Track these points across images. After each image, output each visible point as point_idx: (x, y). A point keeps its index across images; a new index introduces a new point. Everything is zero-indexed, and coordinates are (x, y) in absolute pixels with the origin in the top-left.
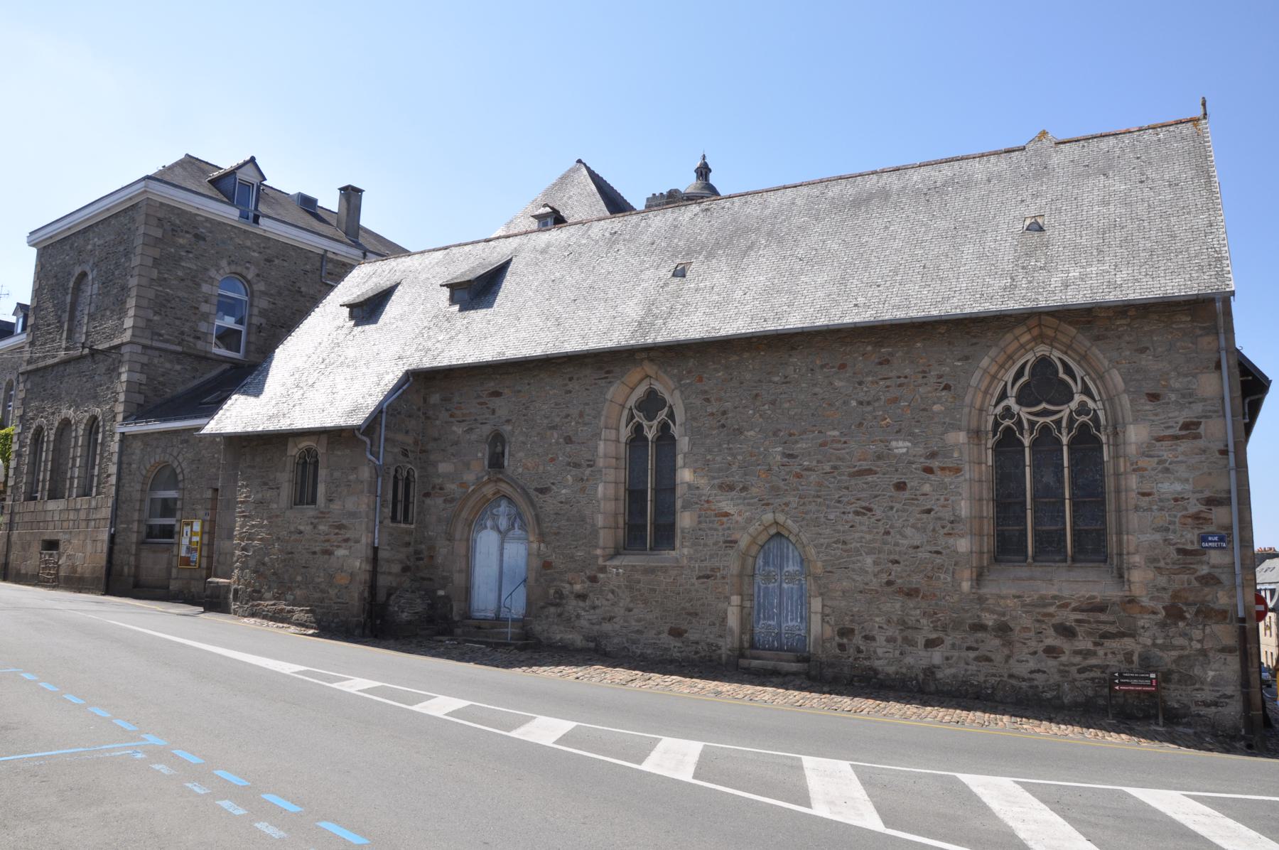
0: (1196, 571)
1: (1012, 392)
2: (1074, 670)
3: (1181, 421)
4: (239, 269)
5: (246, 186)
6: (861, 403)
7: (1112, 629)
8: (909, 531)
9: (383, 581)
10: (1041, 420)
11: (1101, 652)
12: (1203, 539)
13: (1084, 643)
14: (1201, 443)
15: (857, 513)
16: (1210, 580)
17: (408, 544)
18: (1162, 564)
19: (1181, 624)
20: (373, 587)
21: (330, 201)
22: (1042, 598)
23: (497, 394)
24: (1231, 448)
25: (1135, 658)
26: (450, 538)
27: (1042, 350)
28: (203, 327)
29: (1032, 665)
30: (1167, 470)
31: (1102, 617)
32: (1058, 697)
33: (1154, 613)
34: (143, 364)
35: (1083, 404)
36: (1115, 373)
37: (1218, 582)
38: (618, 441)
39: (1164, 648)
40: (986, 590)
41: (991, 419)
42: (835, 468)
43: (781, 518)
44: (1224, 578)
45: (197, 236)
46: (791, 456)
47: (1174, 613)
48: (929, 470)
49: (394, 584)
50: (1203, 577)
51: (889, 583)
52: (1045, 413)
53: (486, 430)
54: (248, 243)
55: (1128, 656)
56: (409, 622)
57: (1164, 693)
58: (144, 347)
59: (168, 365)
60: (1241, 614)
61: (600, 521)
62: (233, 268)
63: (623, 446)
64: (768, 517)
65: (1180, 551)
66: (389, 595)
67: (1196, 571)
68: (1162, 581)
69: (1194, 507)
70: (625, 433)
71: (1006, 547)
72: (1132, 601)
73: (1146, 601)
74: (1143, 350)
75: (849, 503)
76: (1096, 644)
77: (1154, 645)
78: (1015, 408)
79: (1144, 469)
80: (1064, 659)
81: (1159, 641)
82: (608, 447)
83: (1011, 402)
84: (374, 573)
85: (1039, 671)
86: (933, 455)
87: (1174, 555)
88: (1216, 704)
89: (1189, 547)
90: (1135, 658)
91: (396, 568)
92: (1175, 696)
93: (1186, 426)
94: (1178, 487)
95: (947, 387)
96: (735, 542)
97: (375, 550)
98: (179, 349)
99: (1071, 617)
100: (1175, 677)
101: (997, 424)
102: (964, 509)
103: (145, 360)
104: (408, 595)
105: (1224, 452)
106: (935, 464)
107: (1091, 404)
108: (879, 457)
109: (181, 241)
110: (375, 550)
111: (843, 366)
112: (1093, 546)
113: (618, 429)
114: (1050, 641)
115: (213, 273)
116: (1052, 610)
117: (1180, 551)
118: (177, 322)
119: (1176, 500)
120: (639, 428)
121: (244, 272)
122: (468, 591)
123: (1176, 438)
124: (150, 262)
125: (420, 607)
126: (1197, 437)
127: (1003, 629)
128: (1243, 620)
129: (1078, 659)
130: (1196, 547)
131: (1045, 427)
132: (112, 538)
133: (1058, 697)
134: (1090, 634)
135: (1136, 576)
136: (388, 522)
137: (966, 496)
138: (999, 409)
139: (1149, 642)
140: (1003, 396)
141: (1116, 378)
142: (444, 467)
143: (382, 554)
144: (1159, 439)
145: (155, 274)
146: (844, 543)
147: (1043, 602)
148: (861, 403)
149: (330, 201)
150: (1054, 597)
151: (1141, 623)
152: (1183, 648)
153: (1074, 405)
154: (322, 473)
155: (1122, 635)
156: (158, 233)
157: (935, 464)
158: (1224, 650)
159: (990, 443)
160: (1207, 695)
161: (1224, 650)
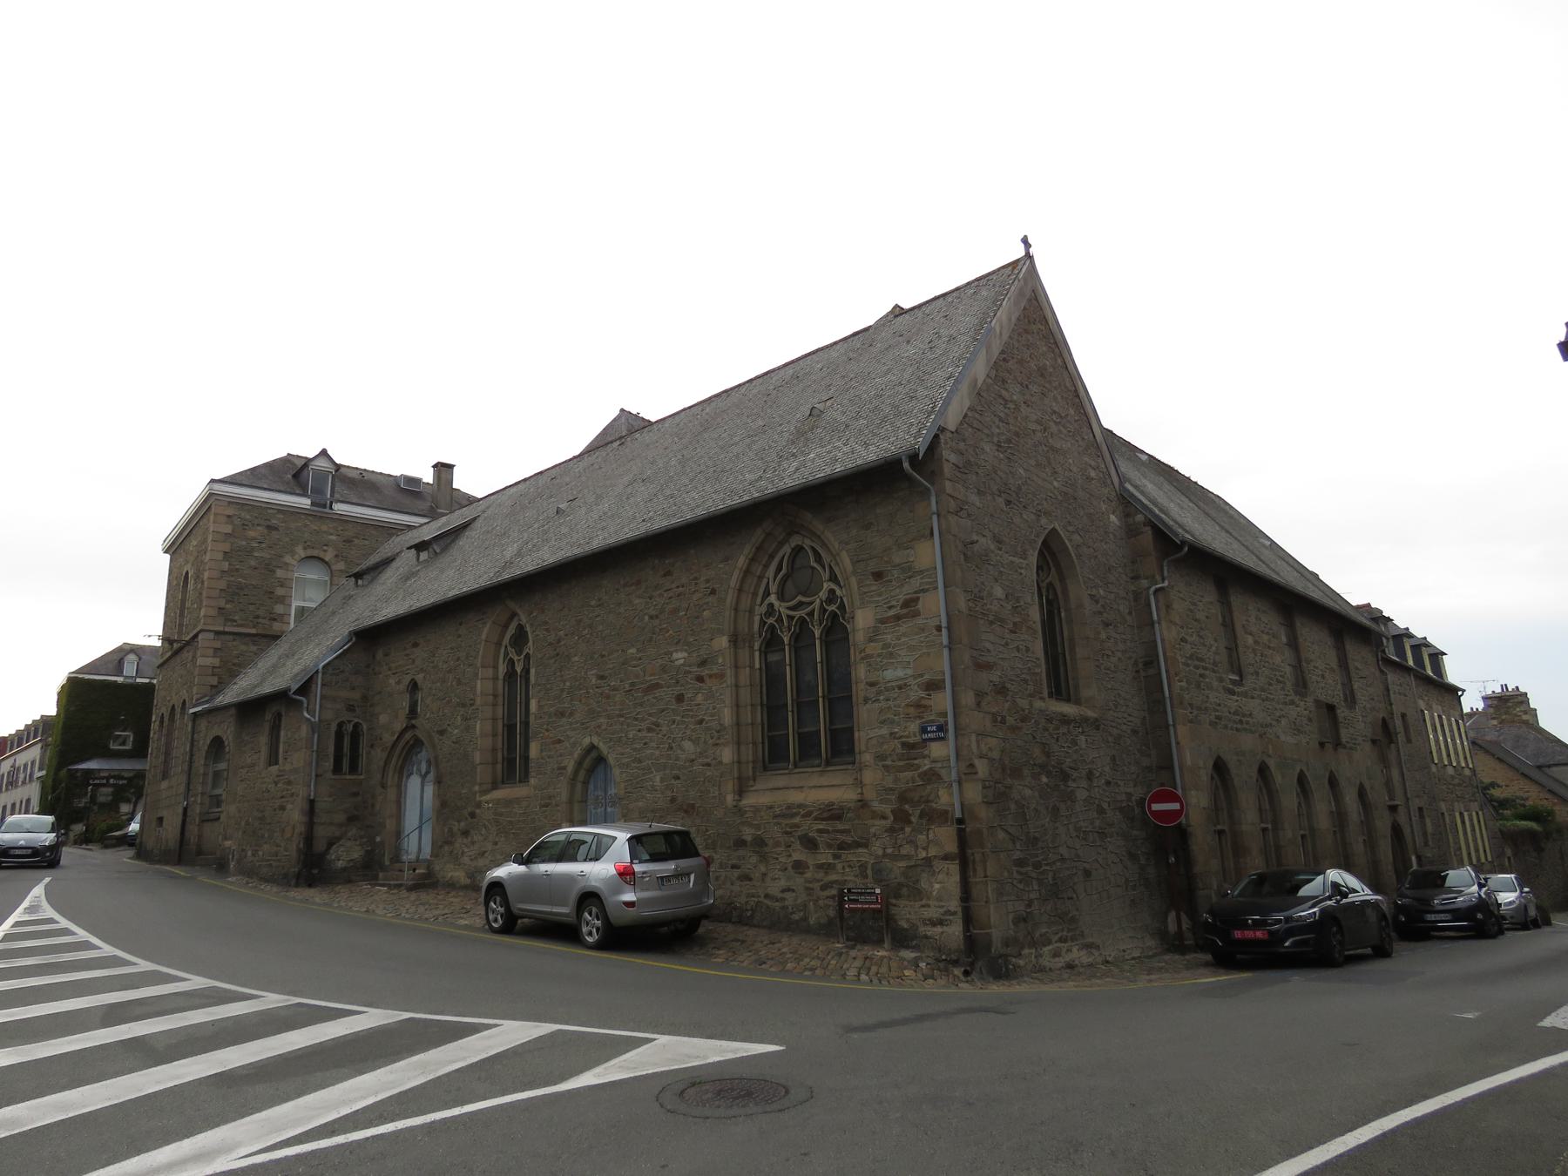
0: (919, 767)
1: (773, 588)
2: (817, 886)
3: (902, 597)
4: (315, 553)
5: (321, 476)
6: (651, 617)
7: (849, 839)
8: (687, 745)
9: (322, 832)
10: (797, 614)
11: (839, 866)
12: (924, 730)
13: (825, 856)
14: (919, 621)
15: (649, 730)
16: (932, 776)
17: (356, 794)
18: (889, 762)
19: (908, 830)
20: (309, 838)
21: (428, 477)
22: (789, 807)
23: (416, 645)
24: (944, 624)
25: (869, 872)
26: (383, 786)
27: (796, 541)
28: (279, 609)
29: (783, 883)
30: (891, 655)
31: (840, 826)
32: (805, 919)
33: (884, 818)
34: (216, 649)
35: (832, 591)
36: (844, 554)
37: (939, 777)
38: (495, 678)
39: (895, 857)
40: (749, 800)
41: (757, 619)
42: (632, 684)
43: (595, 741)
44: (943, 772)
45: (269, 527)
46: (602, 678)
47: (901, 817)
48: (700, 679)
49: (337, 834)
50: (925, 773)
51: (673, 800)
52: (800, 605)
53: (407, 679)
54: (324, 528)
55: (863, 867)
56: (344, 869)
57: (894, 910)
58: (217, 633)
59: (243, 648)
60: (958, 815)
61: (477, 758)
63: (500, 683)
64: (587, 741)
65: (904, 745)
66: (330, 844)
67: (919, 767)
68: (889, 782)
69: (916, 693)
70: (502, 669)
71: (774, 756)
72: (863, 804)
73: (876, 806)
74: (867, 527)
75: (643, 720)
76: (836, 857)
77: (885, 855)
78: (777, 604)
79: (870, 656)
80: (808, 875)
81: (889, 851)
82: (484, 685)
83: (773, 598)
84: (311, 825)
85: (788, 890)
86: (703, 663)
87: (899, 750)
88: (941, 923)
89: (911, 740)
90: (869, 872)
91: (340, 817)
92: (906, 913)
93: (906, 604)
94: (900, 673)
95: (713, 592)
96: (565, 768)
97: (312, 802)
98: (253, 631)
99: (812, 827)
100: (904, 891)
101: (763, 623)
102: (727, 716)
103: (218, 644)
104: (349, 844)
105: (939, 629)
106: (705, 672)
107: (838, 592)
108: (664, 669)
109: (251, 534)
110: (312, 802)
111: (639, 583)
112: (842, 748)
113: (496, 667)
114: (796, 856)
115: (288, 559)
116: (797, 820)
117: (904, 745)
118: (252, 608)
119: (900, 688)
120: (512, 662)
121: (321, 555)
122: (399, 834)
123: (898, 618)
124: (220, 556)
125: (357, 854)
126: (916, 614)
127: (760, 842)
128: (960, 821)
129: (820, 875)
130: (918, 739)
131: (802, 621)
132: (185, 810)
133: (805, 919)
134: (830, 846)
135: (869, 776)
136: (330, 775)
137: (726, 702)
138: (764, 609)
139: (880, 852)
140: (767, 594)
141: (846, 559)
142: (383, 719)
143: (319, 806)
144: (883, 621)
145: (226, 566)
146: (640, 761)
147: (790, 811)
148: (651, 617)
149: (428, 477)
150: (800, 806)
151: (873, 830)
152: (908, 857)
153: (823, 594)
154: (282, 733)
155: (858, 845)
156: (228, 529)
157: (705, 672)
158: (946, 858)
159: (757, 646)
160: (933, 913)
161: (946, 858)
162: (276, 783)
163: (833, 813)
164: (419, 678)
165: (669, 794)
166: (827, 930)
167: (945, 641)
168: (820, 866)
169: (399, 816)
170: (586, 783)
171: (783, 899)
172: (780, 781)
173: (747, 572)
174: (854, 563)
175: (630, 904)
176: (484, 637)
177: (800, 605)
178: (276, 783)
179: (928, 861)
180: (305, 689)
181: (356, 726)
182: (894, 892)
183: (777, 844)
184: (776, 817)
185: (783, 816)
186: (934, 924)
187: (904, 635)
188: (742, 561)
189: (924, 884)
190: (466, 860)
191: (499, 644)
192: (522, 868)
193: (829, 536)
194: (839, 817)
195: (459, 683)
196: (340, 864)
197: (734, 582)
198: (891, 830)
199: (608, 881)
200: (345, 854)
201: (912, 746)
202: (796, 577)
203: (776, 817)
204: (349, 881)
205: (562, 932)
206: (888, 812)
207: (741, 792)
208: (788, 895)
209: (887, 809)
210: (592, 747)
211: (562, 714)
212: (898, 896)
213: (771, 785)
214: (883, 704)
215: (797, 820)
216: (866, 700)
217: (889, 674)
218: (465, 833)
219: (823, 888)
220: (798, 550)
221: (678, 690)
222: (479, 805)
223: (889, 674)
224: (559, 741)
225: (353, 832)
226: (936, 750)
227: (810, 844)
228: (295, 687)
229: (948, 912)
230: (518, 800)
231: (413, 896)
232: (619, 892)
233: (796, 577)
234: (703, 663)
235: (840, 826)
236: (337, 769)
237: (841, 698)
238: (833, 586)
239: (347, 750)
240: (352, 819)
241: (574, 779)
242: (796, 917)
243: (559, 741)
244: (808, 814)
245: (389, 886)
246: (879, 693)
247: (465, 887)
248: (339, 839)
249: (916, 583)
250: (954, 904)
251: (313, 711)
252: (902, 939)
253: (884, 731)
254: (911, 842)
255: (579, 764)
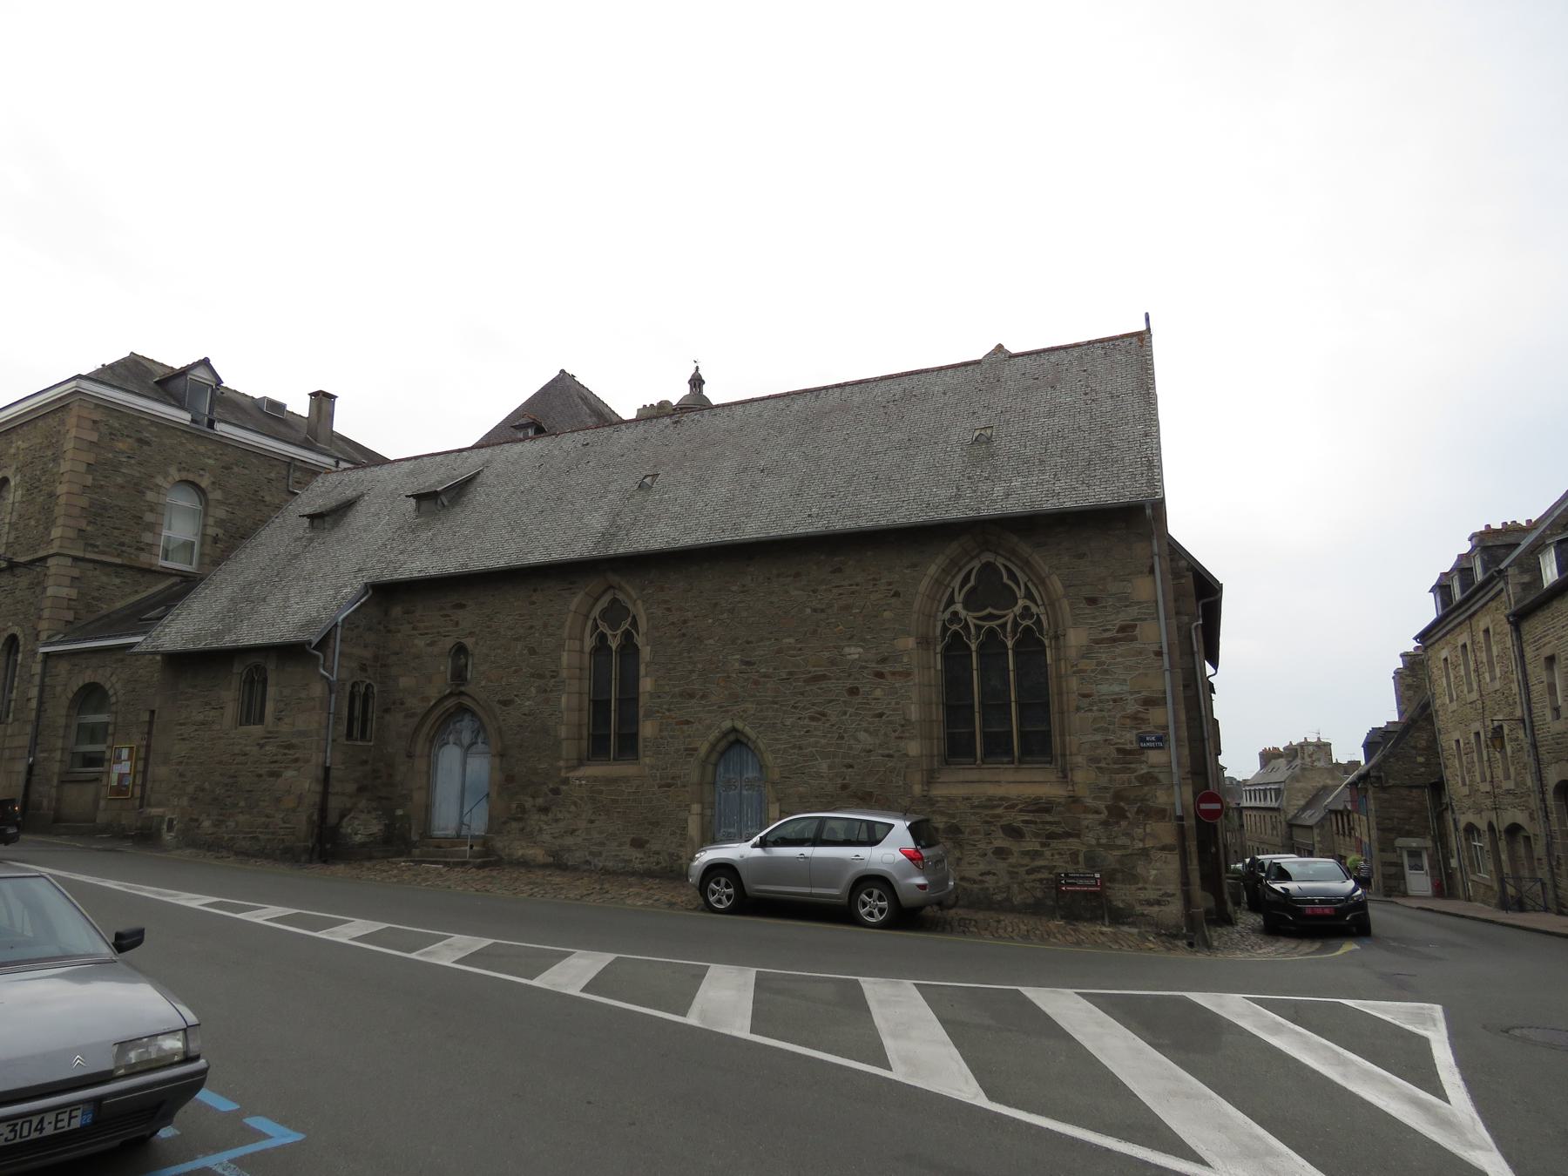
0: (1135, 770)
1: (959, 598)
2: (1022, 870)
3: (1118, 623)
4: (191, 477)
5: (200, 387)
6: (815, 610)
7: (1059, 830)
8: (862, 736)
9: (335, 803)
10: (987, 624)
11: (1048, 854)
12: (1142, 739)
13: (1032, 845)
14: (1136, 645)
15: (812, 719)
16: (1149, 779)
17: (365, 762)
18: (1103, 765)
19: (1124, 823)
20: (323, 809)
21: (299, 406)
22: (990, 799)
23: (462, 606)
24: (1165, 650)
25: (1081, 858)
26: (410, 756)
27: (988, 557)
28: (148, 537)
29: (982, 867)
30: (1106, 672)
31: (1049, 818)
32: (1008, 899)
33: (1097, 812)
34: (74, 579)
35: (1026, 608)
36: (1055, 578)
37: (1157, 781)
38: (582, 651)
39: (1109, 847)
40: (938, 791)
41: (939, 625)
42: (791, 673)
43: (739, 725)
44: (1161, 776)
45: (140, 441)
46: (748, 663)
47: (1116, 813)
48: (880, 675)
49: (349, 805)
50: (1142, 776)
51: (844, 787)
52: (990, 617)
53: (449, 643)
54: (202, 449)
55: (1075, 855)
56: (363, 845)
57: (1109, 892)
58: (75, 559)
59: (104, 579)
60: (1179, 813)
61: (563, 732)
62: (184, 475)
63: (587, 656)
64: (727, 724)
65: (1119, 751)
66: (342, 816)
67: (1135, 770)
68: (1104, 781)
69: (1132, 708)
70: (589, 643)
71: (957, 749)
72: (1074, 800)
73: (1089, 802)
74: (1081, 556)
75: (804, 708)
76: (1043, 845)
77: (1099, 845)
78: (963, 613)
79: (1084, 671)
80: (1012, 860)
81: (1103, 841)
82: (572, 657)
83: (958, 607)
84: (325, 794)
85: (989, 873)
86: (884, 660)
87: (1115, 755)
88: (1158, 903)
89: (1128, 747)
90: (1081, 858)
91: (351, 787)
92: (1121, 894)
93: (1122, 629)
94: (1116, 688)
95: (897, 594)
96: (695, 749)
97: (327, 770)
98: (118, 561)
99: (1018, 819)
100: (1119, 876)
101: (945, 629)
102: (914, 713)
103: (76, 573)
104: (363, 816)
105: (1159, 654)
106: (886, 669)
107: (1034, 609)
108: (833, 662)
109: (120, 446)
110: (327, 770)
111: (797, 575)
112: (1038, 745)
113: (582, 640)
114: (998, 843)
115: (159, 480)
116: (999, 811)
117: (1119, 751)
118: (116, 533)
119: (1115, 701)
120: (603, 637)
121: (197, 480)
122: (428, 808)
123: (1114, 640)
124: (83, 468)
125: (376, 828)
126: (1134, 639)
127: (954, 830)
128: (1181, 818)
129: (1026, 860)
130: (1135, 746)
131: (991, 630)
132: (31, 768)
133: (1008, 899)
134: (1036, 835)
135: (1079, 776)
136: (343, 740)
137: (916, 697)
138: (947, 615)
139: (1094, 842)
140: (951, 601)
141: (1056, 584)
142: (405, 682)
143: (333, 773)
144: (1097, 642)
145: (89, 480)
146: (800, 748)
147: (991, 803)
148: (815, 610)
149: (299, 406)
150: (1002, 799)
151: (1085, 823)
152: (1124, 847)
153: (1017, 609)
154: (271, 691)
155: (1069, 835)
156: (94, 437)
157: (886, 669)
158: (1163, 848)
159: (939, 649)
160: (1152, 894)
161: (1163, 848)
162: (261, 746)
163: (1041, 807)
164: (469, 642)
165: (840, 781)
166: (1035, 909)
167: (1167, 665)
168: (1026, 853)
169: (429, 788)
170: (716, 765)
171: (982, 882)
172: (973, 775)
173: (938, 582)
174: (1066, 587)
175: (922, 887)
176: (573, 607)
177: (990, 617)
178: (261, 746)
179: (1145, 853)
180: (323, 643)
181: (367, 687)
182: (1110, 877)
183: (975, 832)
184: (973, 807)
185: (985, 807)
186: (1150, 903)
187: (1121, 655)
188: (933, 570)
189: (1140, 870)
190: (546, 837)
191: (587, 617)
192: (758, 852)
193: (1037, 559)
194: (1047, 810)
195: (532, 651)
196: (358, 838)
197: (924, 585)
198: (1105, 824)
199: (897, 865)
200: (363, 827)
201: (1130, 752)
202: (989, 591)
203: (973, 807)
204: (370, 858)
205: (840, 913)
206: (1102, 807)
207: (930, 779)
208: (987, 878)
209: (1101, 805)
210: (734, 730)
211: (691, 696)
212: (1112, 880)
213: (961, 778)
214: (1096, 714)
215: (999, 811)
216: (1078, 709)
217: (1104, 688)
218: (544, 810)
219: (1028, 873)
220: (988, 567)
221: (849, 683)
222: (566, 781)
223: (1104, 688)
224: (688, 722)
225: (363, 804)
226: (1155, 757)
227: (1014, 833)
228: (315, 640)
229: (1167, 895)
230: (626, 779)
231: (482, 873)
232: (910, 876)
233: (989, 591)
234: (884, 660)
235: (1049, 818)
236: (349, 735)
237: (1037, 704)
238: (1028, 603)
239: (360, 712)
240: (361, 789)
241: (705, 762)
242: (998, 897)
243: (688, 722)
244: (1013, 806)
245: (446, 864)
246: (1091, 705)
247: (545, 866)
248: (350, 810)
249: (1134, 612)
250: (1173, 887)
251: (336, 668)
252: (1119, 917)
253: (1098, 737)
254: (1127, 835)
255: (713, 747)
